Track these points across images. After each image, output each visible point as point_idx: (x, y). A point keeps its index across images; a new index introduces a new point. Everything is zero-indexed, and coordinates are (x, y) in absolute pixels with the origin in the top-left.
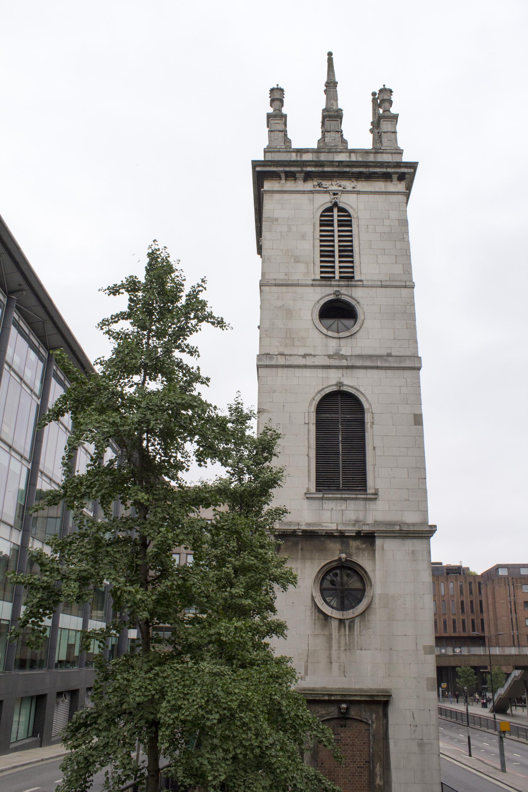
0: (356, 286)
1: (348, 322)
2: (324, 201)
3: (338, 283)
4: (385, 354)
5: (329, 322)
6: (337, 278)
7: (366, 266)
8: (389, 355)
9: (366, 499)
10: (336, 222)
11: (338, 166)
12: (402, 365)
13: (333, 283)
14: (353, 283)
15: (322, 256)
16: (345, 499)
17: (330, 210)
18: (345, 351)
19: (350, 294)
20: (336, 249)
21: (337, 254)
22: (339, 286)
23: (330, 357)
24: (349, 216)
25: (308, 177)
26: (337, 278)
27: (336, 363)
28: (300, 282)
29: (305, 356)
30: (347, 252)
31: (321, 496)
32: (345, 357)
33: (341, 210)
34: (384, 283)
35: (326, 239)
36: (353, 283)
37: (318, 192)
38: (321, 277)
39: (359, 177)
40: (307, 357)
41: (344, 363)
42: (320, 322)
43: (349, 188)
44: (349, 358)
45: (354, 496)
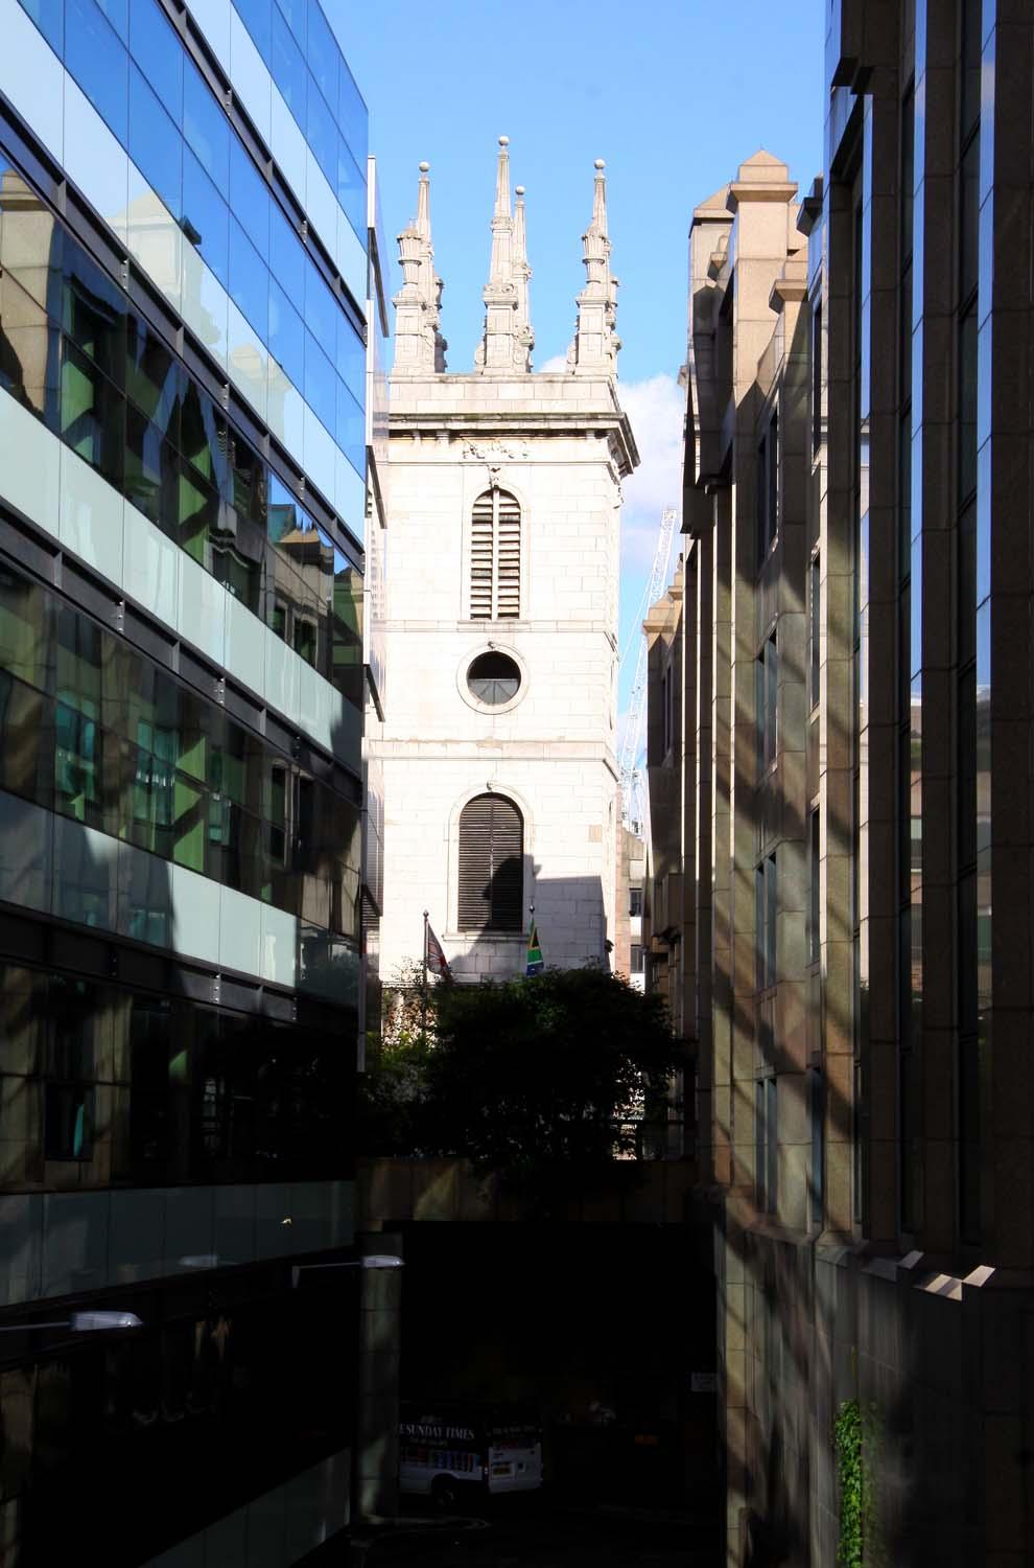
0: (520, 631)
1: (507, 684)
2: (480, 480)
3: (494, 627)
4: (555, 738)
5: (485, 684)
6: (495, 612)
7: (536, 595)
8: (561, 741)
9: (521, 942)
10: (497, 510)
11: (501, 420)
12: (575, 756)
13: (487, 627)
14: (517, 627)
15: (474, 577)
16: (495, 942)
17: (489, 494)
18: (502, 735)
19: (510, 644)
20: (496, 565)
21: (496, 574)
22: (495, 631)
23: (479, 743)
24: (517, 505)
25: (454, 435)
26: (495, 612)
27: (483, 753)
28: (441, 626)
29: (445, 742)
30: (511, 572)
31: (463, 938)
32: (499, 744)
33: (504, 493)
34: (561, 626)
35: (481, 547)
36: (517, 627)
37: (472, 464)
38: (474, 616)
39: (534, 433)
40: (449, 745)
41: (498, 753)
42: (469, 685)
43: (519, 458)
44: (505, 746)
45: (504, 938)
